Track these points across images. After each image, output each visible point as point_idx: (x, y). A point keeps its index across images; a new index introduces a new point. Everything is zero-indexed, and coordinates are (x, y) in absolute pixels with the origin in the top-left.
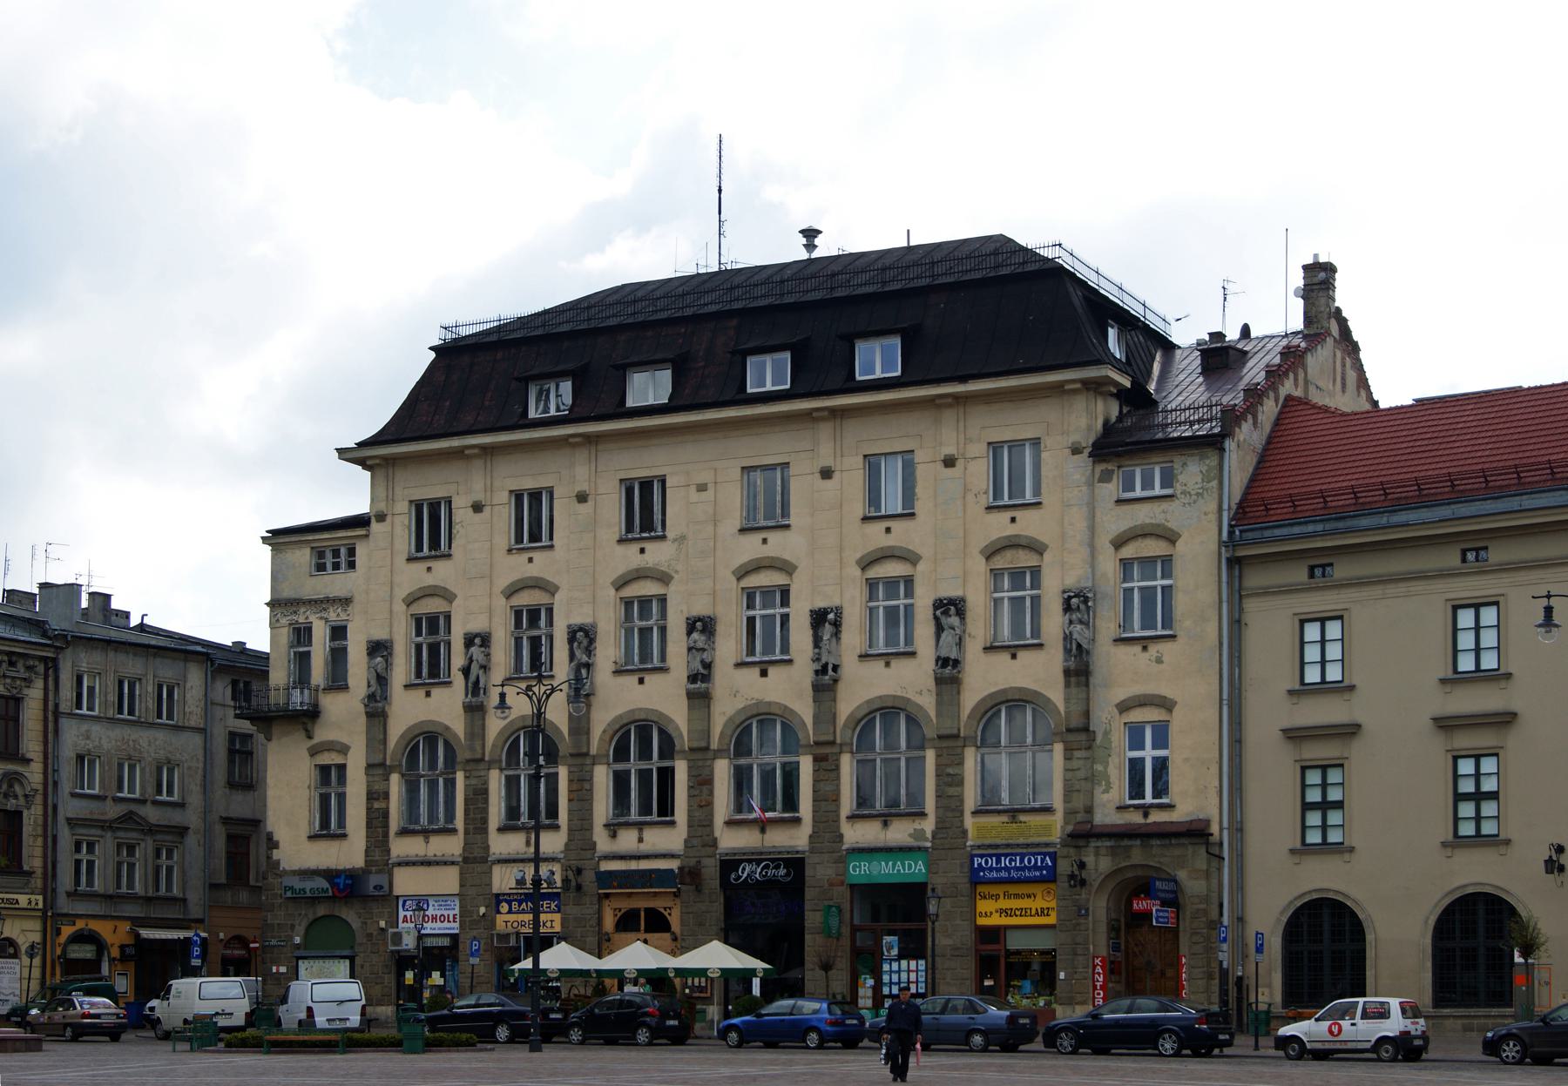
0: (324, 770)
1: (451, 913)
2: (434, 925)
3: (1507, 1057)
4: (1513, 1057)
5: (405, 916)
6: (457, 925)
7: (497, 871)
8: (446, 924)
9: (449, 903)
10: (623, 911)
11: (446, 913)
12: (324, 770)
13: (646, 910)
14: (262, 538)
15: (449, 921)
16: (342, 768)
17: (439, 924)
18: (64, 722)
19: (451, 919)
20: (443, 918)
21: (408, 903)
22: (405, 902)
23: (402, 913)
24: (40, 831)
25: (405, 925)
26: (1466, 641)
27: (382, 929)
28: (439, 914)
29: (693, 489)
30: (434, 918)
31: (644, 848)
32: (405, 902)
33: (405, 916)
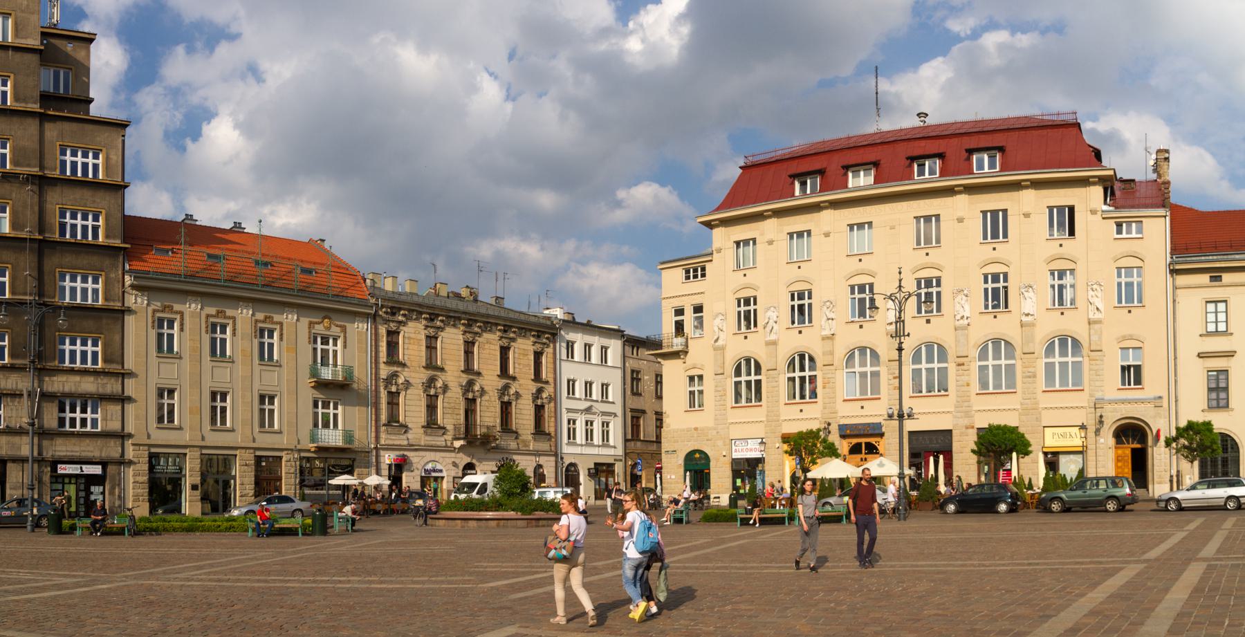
0: (692, 379)
2: (751, 453)
12: (692, 379)
16: (701, 377)
18: (563, 363)
24: (553, 414)
28: (754, 447)
30: (751, 450)
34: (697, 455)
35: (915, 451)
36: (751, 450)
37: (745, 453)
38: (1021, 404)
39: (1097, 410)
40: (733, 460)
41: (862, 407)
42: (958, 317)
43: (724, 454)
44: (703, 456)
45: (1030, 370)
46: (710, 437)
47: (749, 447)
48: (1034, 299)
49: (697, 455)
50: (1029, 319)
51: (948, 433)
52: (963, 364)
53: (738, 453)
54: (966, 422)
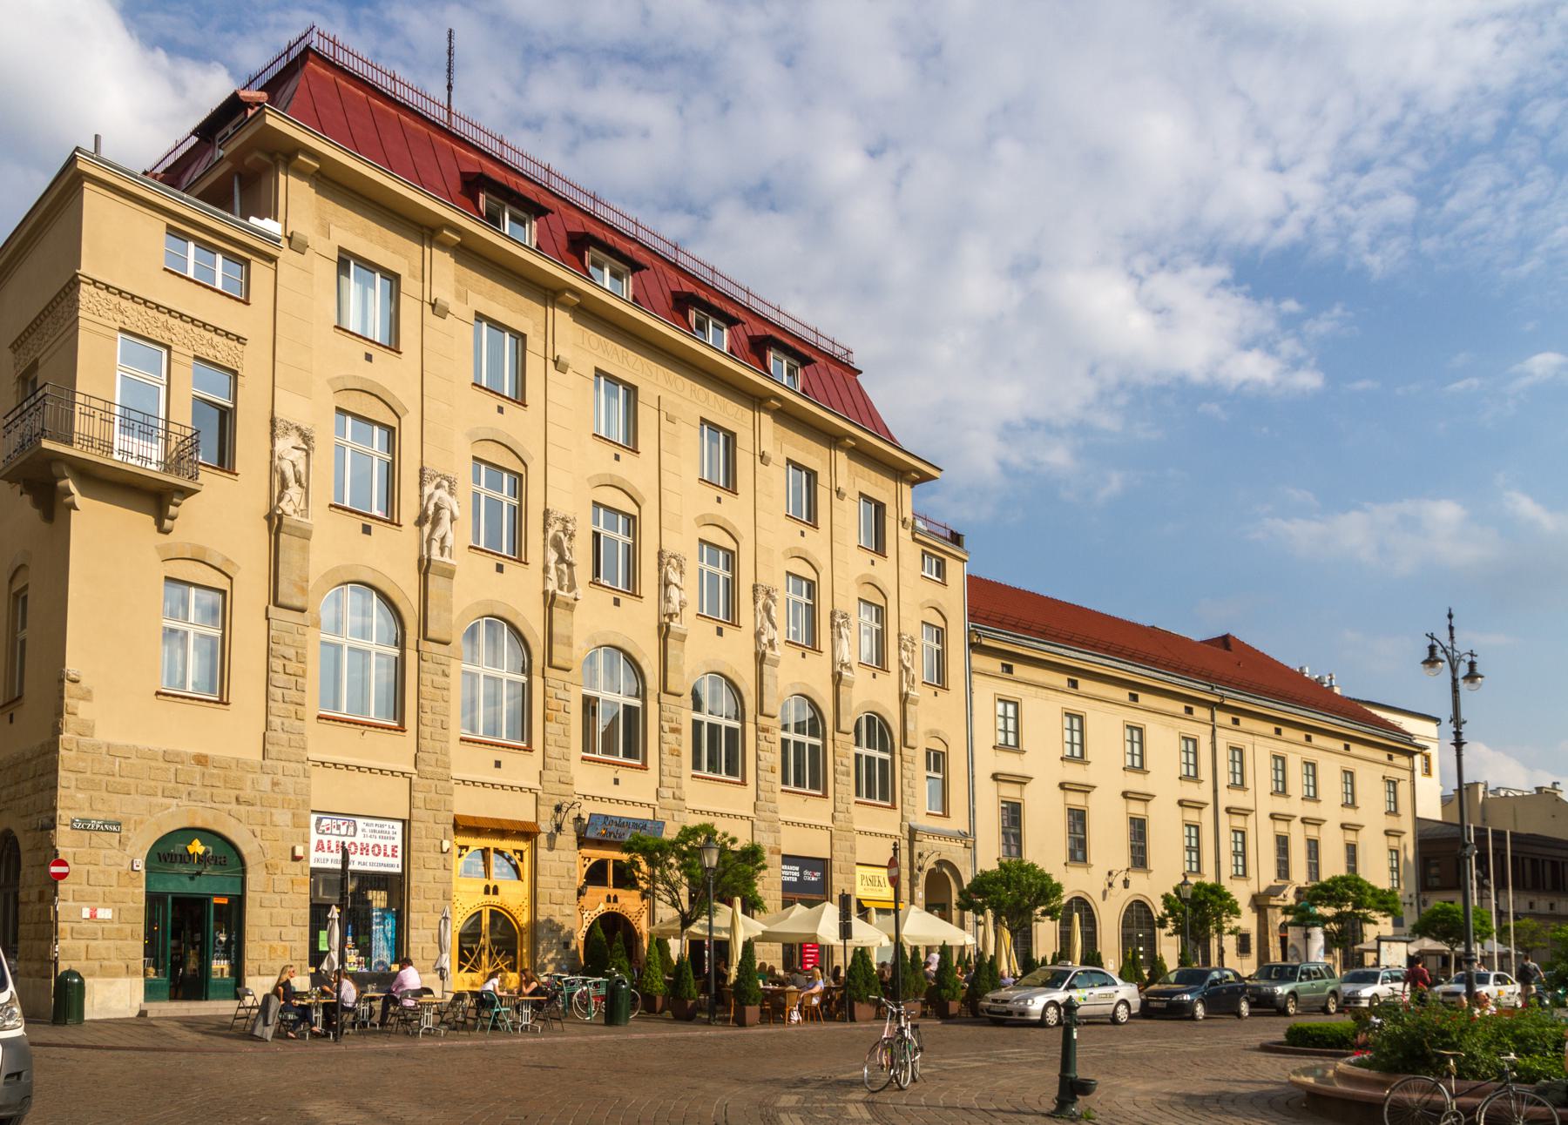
1: (390, 843)
2: (364, 858)
5: (320, 842)
6: (398, 861)
7: (459, 790)
8: (381, 859)
9: (386, 828)
10: (593, 861)
11: (382, 843)
13: (615, 861)
15: (385, 854)
17: (371, 858)
19: (389, 852)
20: (378, 850)
21: (325, 822)
22: (319, 821)
25: (320, 854)
28: (372, 842)
31: (616, 792)
33: (320, 842)
34: (197, 847)
43: (299, 852)
46: (247, 793)
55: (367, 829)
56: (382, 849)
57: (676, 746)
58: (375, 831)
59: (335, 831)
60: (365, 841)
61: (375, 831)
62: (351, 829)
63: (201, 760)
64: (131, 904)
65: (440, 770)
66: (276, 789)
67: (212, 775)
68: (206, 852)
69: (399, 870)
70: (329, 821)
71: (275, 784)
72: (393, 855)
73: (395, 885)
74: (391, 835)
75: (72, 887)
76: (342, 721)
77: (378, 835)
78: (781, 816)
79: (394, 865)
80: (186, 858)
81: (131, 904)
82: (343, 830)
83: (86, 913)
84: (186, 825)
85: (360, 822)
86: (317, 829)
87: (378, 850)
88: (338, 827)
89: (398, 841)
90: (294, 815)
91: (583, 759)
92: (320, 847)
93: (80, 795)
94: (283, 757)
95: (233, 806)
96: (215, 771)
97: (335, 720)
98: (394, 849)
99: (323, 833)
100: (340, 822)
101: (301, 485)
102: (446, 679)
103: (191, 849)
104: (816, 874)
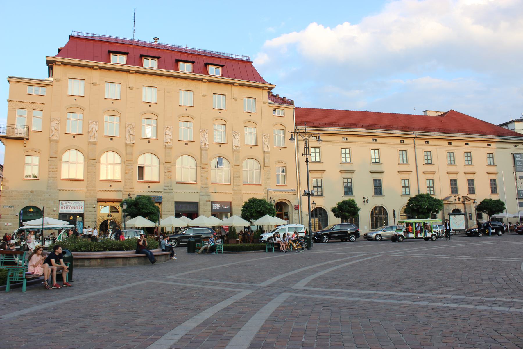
1: (80, 206)
3: (378, 239)
4: (380, 238)
8: (78, 210)
9: (79, 203)
11: (78, 206)
14: (7, 78)
15: (79, 209)
17: (75, 210)
19: (80, 208)
20: (77, 208)
21: (63, 203)
22: (62, 202)
23: (61, 206)
25: (62, 210)
26: (348, 156)
27: (55, 211)
28: (75, 206)
29: (166, 92)
30: (74, 208)
32: (62, 202)
34: (31, 210)
35: (178, 213)
36: (74, 208)
37: (69, 210)
38: (233, 190)
39: (269, 195)
40: (60, 214)
41: (111, 186)
42: (203, 144)
43: (55, 209)
44: (35, 210)
45: (238, 173)
47: (72, 206)
48: (239, 140)
49: (31, 210)
50: (237, 148)
51: (197, 203)
52: (205, 168)
53: (64, 210)
54: (206, 198)
55: (74, 203)
56: (78, 207)
57: (170, 176)
58: (76, 204)
59: (66, 204)
60: (74, 206)
61: (76, 204)
62: (70, 204)
63: (32, 192)
64: (16, 222)
65: (93, 189)
66: (50, 196)
67: (34, 195)
68: (33, 211)
69: (83, 212)
70: (64, 202)
71: (50, 195)
72: (81, 209)
73: (82, 215)
74: (81, 204)
75: (3, 219)
76: (248, 185)
77: (77, 205)
78: (210, 191)
79: (81, 211)
80: (29, 212)
81: (16, 222)
82: (68, 204)
83: (6, 224)
84: (28, 205)
85: (72, 202)
86: (61, 204)
87: (77, 208)
88: (67, 203)
89: (83, 206)
90: (54, 202)
91: (138, 182)
92: (62, 208)
93: (5, 201)
94: (51, 189)
95: (39, 201)
96: (35, 194)
97: (247, 185)
98: (82, 208)
99: (63, 205)
100: (67, 202)
101: (52, 129)
102: (95, 168)
103: (30, 210)
104: (227, 206)
